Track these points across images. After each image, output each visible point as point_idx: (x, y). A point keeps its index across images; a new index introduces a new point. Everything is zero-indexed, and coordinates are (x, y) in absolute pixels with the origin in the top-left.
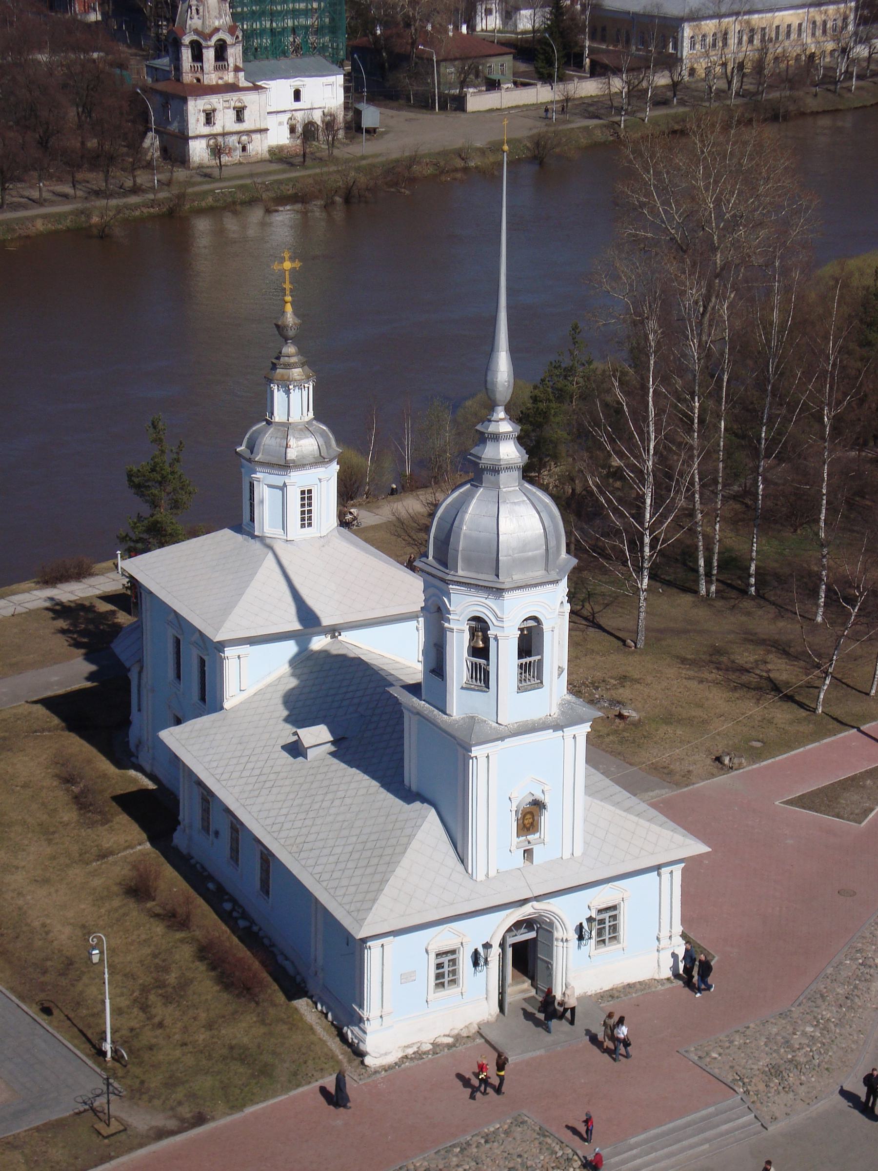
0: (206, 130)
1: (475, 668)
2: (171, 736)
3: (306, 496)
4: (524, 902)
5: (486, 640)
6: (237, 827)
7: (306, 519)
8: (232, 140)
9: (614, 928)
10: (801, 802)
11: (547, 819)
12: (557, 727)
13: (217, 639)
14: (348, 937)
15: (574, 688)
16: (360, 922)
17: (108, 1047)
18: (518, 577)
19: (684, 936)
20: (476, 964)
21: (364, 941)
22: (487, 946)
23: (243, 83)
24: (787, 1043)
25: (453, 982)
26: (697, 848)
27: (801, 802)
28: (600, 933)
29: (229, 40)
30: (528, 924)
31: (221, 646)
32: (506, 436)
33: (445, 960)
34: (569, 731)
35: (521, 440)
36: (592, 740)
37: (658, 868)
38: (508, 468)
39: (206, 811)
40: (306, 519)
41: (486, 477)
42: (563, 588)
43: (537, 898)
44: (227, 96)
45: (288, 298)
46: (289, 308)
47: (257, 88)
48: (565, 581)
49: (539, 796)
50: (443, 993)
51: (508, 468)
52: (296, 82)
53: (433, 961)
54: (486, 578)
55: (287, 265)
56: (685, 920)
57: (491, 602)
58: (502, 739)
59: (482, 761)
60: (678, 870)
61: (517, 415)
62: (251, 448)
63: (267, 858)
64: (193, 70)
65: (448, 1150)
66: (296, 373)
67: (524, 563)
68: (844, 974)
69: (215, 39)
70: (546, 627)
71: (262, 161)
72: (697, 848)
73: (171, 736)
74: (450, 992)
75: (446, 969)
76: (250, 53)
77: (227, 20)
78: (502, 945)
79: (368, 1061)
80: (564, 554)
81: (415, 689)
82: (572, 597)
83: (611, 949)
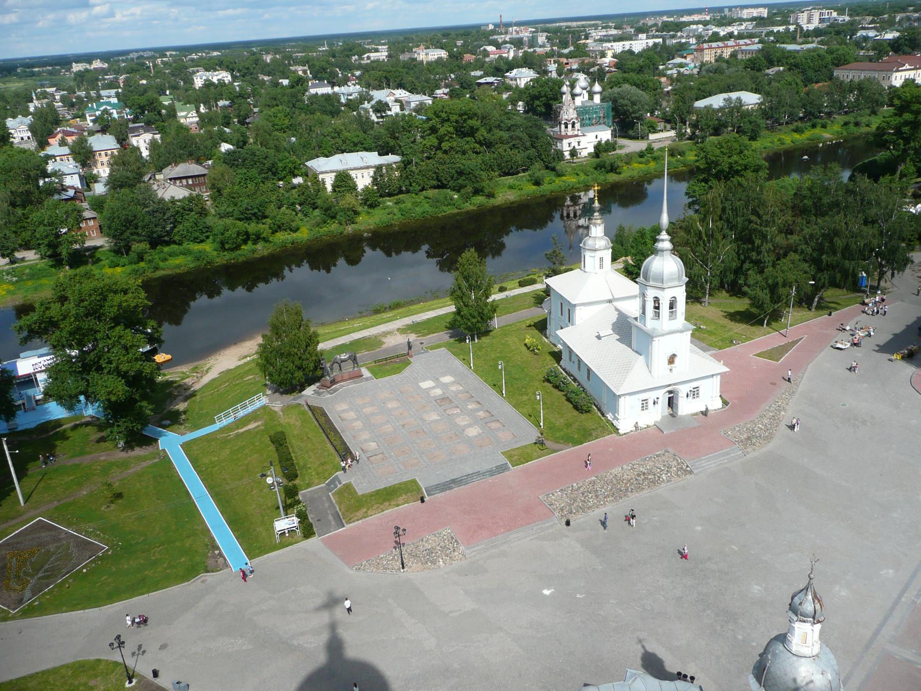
0: (569, 149)
2: (560, 333)
3: (601, 259)
4: (670, 385)
5: (659, 304)
6: (580, 361)
7: (601, 266)
9: (698, 394)
10: (758, 355)
11: (676, 360)
12: (681, 332)
13: (573, 303)
14: (614, 394)
15: (687, 319)
16: (618, 390)
17: (542, 424)
18: (670, 284)
19: (720, 396)
20: (654, 403)
21: (620, 396)
22: (658, 398)
23: (580, 134)
24: (753, 430)
26: (726, 369)
27: (758, 355)
28: (694, 395)
29: (576, 121)
30: (670, 392)
31: (575, 306)
32: (666, 240)
33: (644, 402)
34: (685, 333)
35: (671, 241)
36: (692, 335)
37: (713, 375)
39: (570, 356)
40: (601, 266)
41: (660, 253)
42: (684, 287)
43: (674, 384)
46: (596, 201)
47: (584, 135)
48: (684, 286)
50: (643, 412)
52: (596, 133)
53: (641, 402)
54: (659, 285)
56: (721, 392)
57: (661, 292)
58: (663, 335)
59: (657, 341)
60: (719, 377)
61: (668, 233)
62: (584, 244)
63: (589, 370)
65: (645, 459)
66: (599, 221)
67: (671, 280)
68: (772, 409)
70: (678, 300)
71: (585, 157)
72: (726, 369)
73: (560, 333)
74: (645, 411)
76: (582, 125)
77: (576, 116)
79: (620, 431)
80: (684, 277)
81: (636, 319)
82: (686, 291)
83: (697, 399)
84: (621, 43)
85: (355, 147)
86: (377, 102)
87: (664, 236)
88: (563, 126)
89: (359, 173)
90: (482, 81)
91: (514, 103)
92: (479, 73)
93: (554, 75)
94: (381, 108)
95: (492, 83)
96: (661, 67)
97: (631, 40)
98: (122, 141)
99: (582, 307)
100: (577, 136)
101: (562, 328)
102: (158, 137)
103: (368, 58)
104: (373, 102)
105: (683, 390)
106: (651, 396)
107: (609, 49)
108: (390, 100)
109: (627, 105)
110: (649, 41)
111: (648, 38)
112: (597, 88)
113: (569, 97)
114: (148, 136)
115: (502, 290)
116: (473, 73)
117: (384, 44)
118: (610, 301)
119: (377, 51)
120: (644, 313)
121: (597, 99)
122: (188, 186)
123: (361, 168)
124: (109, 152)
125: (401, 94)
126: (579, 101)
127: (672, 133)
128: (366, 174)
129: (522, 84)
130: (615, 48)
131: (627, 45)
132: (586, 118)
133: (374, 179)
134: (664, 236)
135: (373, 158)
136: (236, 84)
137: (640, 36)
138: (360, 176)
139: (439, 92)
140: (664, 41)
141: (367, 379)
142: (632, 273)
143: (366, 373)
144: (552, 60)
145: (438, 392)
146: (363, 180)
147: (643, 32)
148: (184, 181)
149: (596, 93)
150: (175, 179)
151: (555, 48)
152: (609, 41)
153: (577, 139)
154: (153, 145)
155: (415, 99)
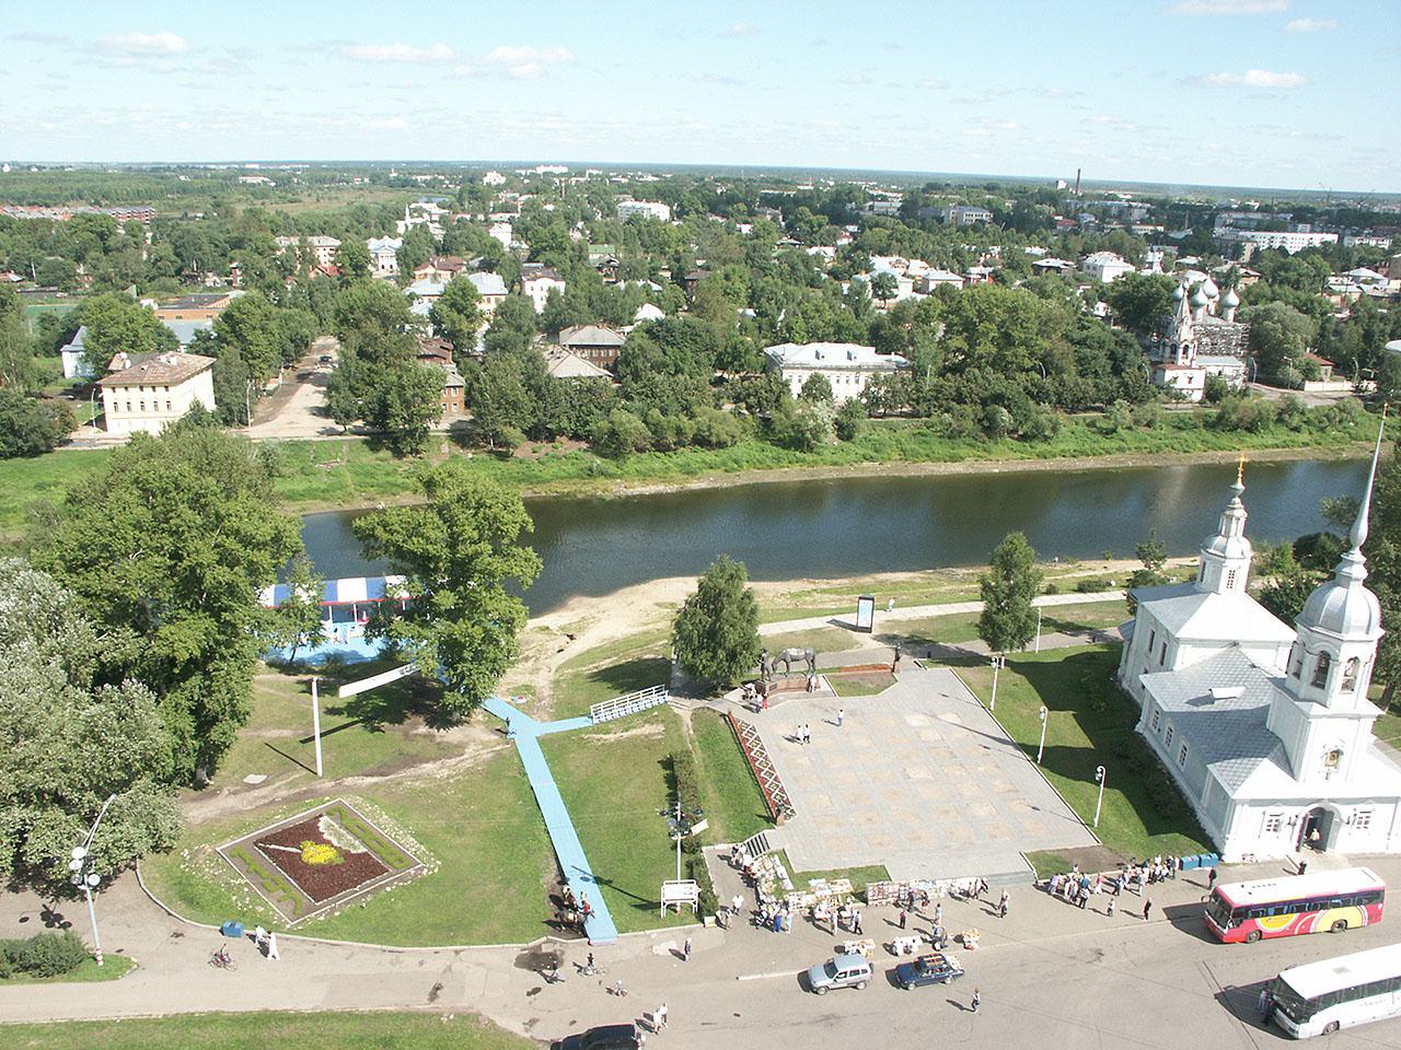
1: (1317, 678)
3: (1232, 574)
8: (1184, 392)
9: (1366, 823)
14: (1226, 797)
25: (1275, 830)
29: (1191, 346)
32: (1358, 563)
33: (1274, 818)
38: (1357, 580)
42: (1374, 645)
44: (1185, 371)
45: (1240, 475)
46: (1240, 480)
49: (1339, 747)
51: (1357, 580)
55: (1243, 460)
64: (1170, 357)
69: (1182, 346)
75: (1273, 823)
77: (1192, 337)
78: (1304, 819)
79: (1223, 858)
84: (1270, 234)
85: (839, 335)
86: (880, 276)
87: (1357, 555)
88: (1168, 350)
89: (844, 375)
90: (1042, 263)
91: (1090, 303)
92: (1037, 251)
93: (1157, 269)
94: (883, 286)
95: (1058, 269)
96: (1332, 280)
97: (1285, 230)
98: (514, 282)
99: (1189, 647)
100: (1190, 368)
101: (1146, 672)
102: (561, 286)
103: (871, 208)
104: (876, 274)
105: (1345, 812)
106: (1290, 812)
107: (1248, 240)
108: (897, 273)
109: (1275, 329)
110: (1314, 236)
111: (1312, 231)
112: (1233, 299)
113: (1186, 307)
114: (547, 283)
115: (1051, 591)
116: (1028, 250)
117: (895, 191)
118: (1235, 644)
119: (884, 199)
120: (1297, 675)
121: (1231, 313)
122: (592, 359)
123: (847, 369)
124: (493, 298)
125: (917, 267)
126: (1200, 312)
127: (1347, 386)
128: (852, 379)
129: (1107, 278)
130: (1258, 240)
131: (1277, 239)
132: (1213, 345)
133: (868, 388)
134: (1357, 555)
135: (867, 355)
136: (675, 223)
137: (1300, 226)
138: (843, 379)
139: (975, 271)
140: (1341, 239)
141: (825, 694)
142: (1281, 605)
143: (825, 686)
144: (1155, 248)
145: (932, 735)
146: (846, 389)
147: (1305, 221)
148: (595, 353)
149: (1230, 306)
150: (578, 347)
151: (1161, 229)
152: (1248, 229)
153: (1189, 373)
154: (552, 297)
155: (937, 277)
